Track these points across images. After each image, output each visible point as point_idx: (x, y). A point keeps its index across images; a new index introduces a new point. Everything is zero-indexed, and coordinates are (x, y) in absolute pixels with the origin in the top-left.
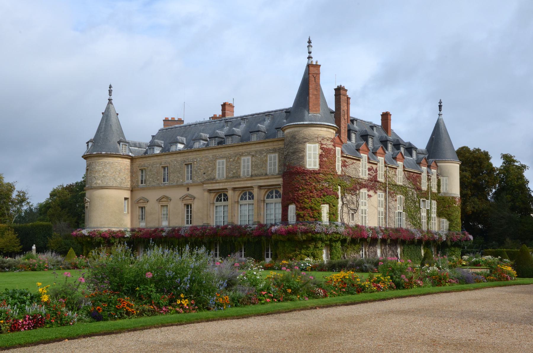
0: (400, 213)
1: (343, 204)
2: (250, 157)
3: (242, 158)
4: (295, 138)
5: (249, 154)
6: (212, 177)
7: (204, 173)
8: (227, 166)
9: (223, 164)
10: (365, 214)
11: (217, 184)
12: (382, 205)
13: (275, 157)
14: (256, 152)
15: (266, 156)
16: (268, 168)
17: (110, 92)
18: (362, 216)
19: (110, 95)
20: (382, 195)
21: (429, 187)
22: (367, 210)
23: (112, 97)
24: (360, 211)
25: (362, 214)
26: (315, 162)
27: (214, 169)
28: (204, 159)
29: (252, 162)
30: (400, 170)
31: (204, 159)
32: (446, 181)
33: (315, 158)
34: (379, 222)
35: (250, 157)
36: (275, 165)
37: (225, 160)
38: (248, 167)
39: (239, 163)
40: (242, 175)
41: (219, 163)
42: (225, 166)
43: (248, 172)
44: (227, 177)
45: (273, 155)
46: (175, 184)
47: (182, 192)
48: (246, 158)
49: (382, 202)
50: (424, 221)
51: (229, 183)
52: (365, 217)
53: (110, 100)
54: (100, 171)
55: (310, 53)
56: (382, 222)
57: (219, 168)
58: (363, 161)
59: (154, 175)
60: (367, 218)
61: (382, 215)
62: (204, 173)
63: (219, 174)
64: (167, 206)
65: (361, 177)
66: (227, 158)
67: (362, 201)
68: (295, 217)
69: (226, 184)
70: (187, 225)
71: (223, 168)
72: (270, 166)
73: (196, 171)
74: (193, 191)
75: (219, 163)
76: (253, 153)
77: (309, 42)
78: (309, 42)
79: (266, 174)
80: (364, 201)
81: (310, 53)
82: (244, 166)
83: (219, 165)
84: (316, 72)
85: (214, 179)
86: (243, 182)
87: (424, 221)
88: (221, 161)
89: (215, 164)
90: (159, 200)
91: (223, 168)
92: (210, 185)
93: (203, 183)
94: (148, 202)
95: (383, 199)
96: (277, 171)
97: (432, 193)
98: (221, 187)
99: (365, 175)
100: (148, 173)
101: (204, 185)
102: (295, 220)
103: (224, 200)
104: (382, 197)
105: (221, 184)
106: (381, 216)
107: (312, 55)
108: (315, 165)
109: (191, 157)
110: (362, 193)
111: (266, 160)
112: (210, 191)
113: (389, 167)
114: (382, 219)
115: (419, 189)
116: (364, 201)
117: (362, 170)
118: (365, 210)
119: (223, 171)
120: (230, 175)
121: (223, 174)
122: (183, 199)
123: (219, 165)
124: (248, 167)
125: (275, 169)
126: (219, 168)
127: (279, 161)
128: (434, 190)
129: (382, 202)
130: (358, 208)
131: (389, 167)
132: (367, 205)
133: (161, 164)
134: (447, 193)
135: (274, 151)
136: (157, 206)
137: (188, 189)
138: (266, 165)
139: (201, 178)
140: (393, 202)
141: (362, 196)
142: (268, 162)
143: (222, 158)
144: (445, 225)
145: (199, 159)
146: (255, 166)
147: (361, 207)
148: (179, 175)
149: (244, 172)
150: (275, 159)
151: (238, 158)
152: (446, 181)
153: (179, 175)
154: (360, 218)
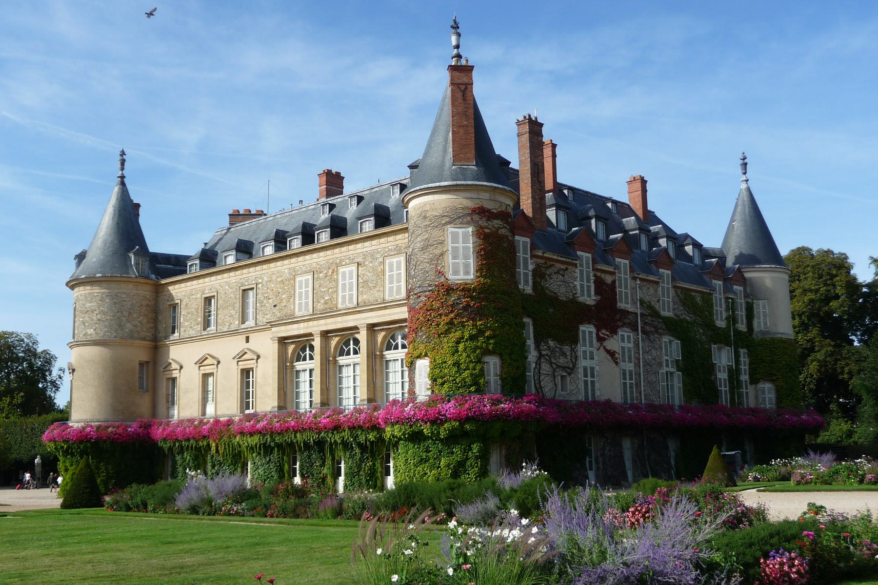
0: (672, 373)
1: (540, 356)
7: (275, 306)
10: (593, 376)
11: (295, 326)
12: (630, 357)
13: (399, 263)
14: (365, 256)
15: (384, 262)
17: (123, 162)
18: (586, 382)
19: (122, 169)
20: (629, 337)
21: (732, 319)
22: (597, 368)
24: (581, 371)
25: (586, 376)
26: (466, 266)
28: (274, 277)
30: (667, 285)
32: (764, 307)
33: (466, 257)
34: (625, 393)
39: (337, 281)
45: (395, 260)
47: (237, 344)
48: (346, 269)
49: (629, 351)
50: (724, 389)
51: (315, 323)
52: (593, 382)
56: (632, 392)
58: (582, 266)
60: (597, 385)
61: (631, 379)
62: (275, 306)
65: (581, 299)
67: (584, 348)
69: (311, 323)
75: (301, 282)
76: (360, 260)
80: (588, 349)
84: (465, 80)
85: (292, 315)
87: (723, 389)
90: (201, 362)
93: (272, 324)
95: (631, 345)
97: (737, 333)
98: (302, 332)
99: (589, 295)
104: (629, 342)
105: (302, 325)
106: (628, 381)
108: (467, 273)
110: (584, 332)
111: (383, 271)
112: (283, 341)
113: (641, 279)
114: (631, 387)
115: (709, 325)
116: (588, 349)
117: (582, 286)
118: (592, 369)
120: (320, 306)
122: (240, 357)
126: (301, 293)
128: (742, 327)
129: (629, 351)
130: (574, 365)
131: (641, 279)
132: (596, 358)
133: (203, 293)
134: (768, 332)
135: (398, 251)
139: (268, 317)
140: (653, 351)
141: (584, 340)
142: (387, 274)
143: (306, 272)
144: (767, 396)
145: (266, 279)
147: (583, 363)
148: (233, 312)
149: (344, 297)
152: (764, 307)
154: (582, 386)
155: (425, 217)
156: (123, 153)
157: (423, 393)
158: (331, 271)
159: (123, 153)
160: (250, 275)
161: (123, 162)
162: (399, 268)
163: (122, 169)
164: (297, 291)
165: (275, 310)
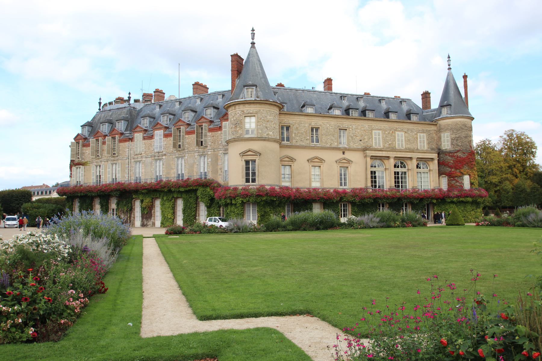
2: (403, 133)
3: (397, 133)
5: (402, 131)
6: (369, 145)
8: (383, 137)
9: (379, 135)
11: (380, 152)
13: (423, 136)
14: (408, 130)
15: (417, 134)
16: (419, 144)
19: (253, 39)
23: (255, 41)
27: (370, 138)
28: (359, 127)
29: (405, 137)
31: (359, 127)
36: (424, 143)
37: (380, 132)
38: (402, 141)
39: (395, 137)
40: (397, 147)
41: (375, 133)
43: (402, 145)
44: (384, 146)
45: (422, 135)
46: (328, 146)
47: (339, 155)
48: (400, 133)
51: (391, 153)
53: (253, 44)
54: (272, 122)
55: (449, 65)
57: (376, 138)
59: (302, 134)
63: (376, 143)
64: (320, 166)
66: (384, 130)
68: (469, 185)
69: (389, 153)
70: (341, 187)
71: (379, 138)
72: (420, 143)
73: (352, 137)
74: (349, 155)
75: (375, 133)
77: (449, 57)
78: (449, 57)
79: (418, 149)
81: (449, 65)
82: (398, 140)
83: (375, 135)
86: (404, 153)
88: (377, 132)
89: (371, 134)
91: (379, 138)
92: (373, 152)
94: (308, 160)
96: (426, 148)
100: (295, 132)
101: (367, 152)
102: (469, 187)
103: (378, 167)
105: (384, 152)
107: (451, 67)
112: (373, 158)
119: (379, 140)
120: (387, 145)
123: (375, 135)
125: (424, 146)
133: (310, 125)
135: (423, 132)
137: (344, 153)
138: (417, 141)
142: (419, 139)
146: (408, 141)
149: (399, 144)
151: (393, 132)
155: (466, 126)
156: (253, 30)
157: (444, 186)
158: (391, 132)
159: (253, 30)
160: (346, 123)
161: (253, 35)
162: (423, 138)
163: (253, 39)
164: (374, 136)
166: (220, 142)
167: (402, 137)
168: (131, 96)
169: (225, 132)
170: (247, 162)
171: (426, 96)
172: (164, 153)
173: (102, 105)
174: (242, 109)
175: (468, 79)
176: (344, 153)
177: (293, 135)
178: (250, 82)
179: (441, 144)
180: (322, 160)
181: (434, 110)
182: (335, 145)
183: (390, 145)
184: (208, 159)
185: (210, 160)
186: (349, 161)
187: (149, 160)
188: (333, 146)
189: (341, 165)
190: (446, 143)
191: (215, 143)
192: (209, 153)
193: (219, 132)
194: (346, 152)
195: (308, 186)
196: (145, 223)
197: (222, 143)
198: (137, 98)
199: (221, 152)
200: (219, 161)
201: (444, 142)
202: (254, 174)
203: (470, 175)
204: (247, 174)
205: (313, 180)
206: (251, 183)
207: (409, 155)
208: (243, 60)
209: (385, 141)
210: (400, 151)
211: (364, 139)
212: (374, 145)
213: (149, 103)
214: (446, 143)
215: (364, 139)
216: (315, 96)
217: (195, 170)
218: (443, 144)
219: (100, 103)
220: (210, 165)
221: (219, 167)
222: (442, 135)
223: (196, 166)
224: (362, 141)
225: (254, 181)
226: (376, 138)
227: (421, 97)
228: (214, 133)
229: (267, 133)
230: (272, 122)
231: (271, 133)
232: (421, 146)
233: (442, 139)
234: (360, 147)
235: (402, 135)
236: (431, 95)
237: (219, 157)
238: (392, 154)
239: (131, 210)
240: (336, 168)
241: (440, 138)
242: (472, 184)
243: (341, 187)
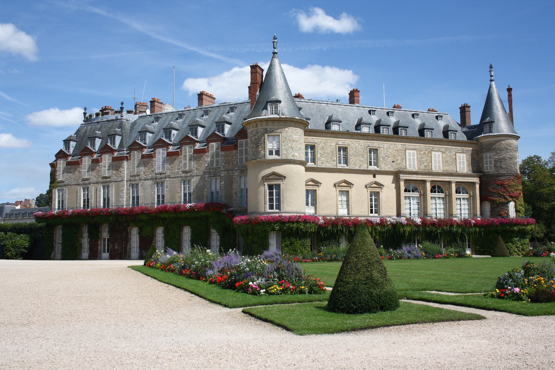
3: (433, 153)
4: (511, 146)
6: (403, 167)
7: (393, 162)
8: (417, 158)
9: (414, 156)
13: (463, 157)
29: (443, 158)
35: (440, 153)
36: (463, 164)
37: (415, 152)
38: (439, 163)
41: (410, 153)
42: (416, 157)
43: (439, 167)
45: (461, 155)
46: (357, 168)
47: (369, 178)
54: (297, 141)
57: (410, 159)
62: (393, 162)
71: (414, 159)
72: (460, 164)
73: (383, 158)
74: (380, 178)
75: (410, 153)
76: (443, 150)
77: (491, 67)
78: (491, 67)
82: (435, 161)
83: (409, 156)
88: (411, 152)
91: (414, 159)
100: (320, 152)
109: (375, 144)
120: (422, 167)
121: (414, 165)
124: (439, 163)
125: (464, 168)
127: (467, 161)
136: (334, 192)
137: (374, 177)
139: (389, 166)
146: (445, 162)
148: (363, 159)
149: (435, 166)
150: (463, 159)
151: (429, 152)
153: (363, 159)
158: (427, 152)
162: (463, 159)
164: (407, 157)
165: (393, 164)
166: (235, 163)
167: (439, 158)
168: (123, 106)
169: (241, 151)
170: (271, 187)
171: (464, 110)
172: (168, 174)
173: (87, 115)
174: (265, 127)
175: (513, 92)
176: (374, 177)
177: (319, 156)
178: (274, 97)
179: (483, 166)
180: (349, 184)
181: (475, 127)
182: (364, 167)
183: (425, 166)
184: (220, 182)
185: (223, 183)
186: (380, 185)
187: (149, 182)
188: (362, 168)
189: (372, 190)
190: (489, 165)
191: (229, 164)
192: (222, 175)
193: (234, 151)
194: (377, 176)
195: (335, 214)
196: (144, 255)
197: (237, 163)
198: (130, 109)
199: (236, 174)
200: (234, 184)
201: (487, 164)
202: (279, 200)
203: (515, 202)
204: (271, 200)
205: (340, 206)
206: (275, 210)
207: (447, 179)
208: (263, 70)
209: (420, 162)
210: (438, 174)
211: (397, 160)
212: (408, 167)
213: (144, 114)
214: (489, 165)
215: (397, 160)
216: (340, 110)
217: (205, 194)
218: (485, 166)
219: (85, 114)
220: (223, 188)
221: (234, 191)
222: (484, 155)
223: (206, 190)
224: (395, 163)
225: (278, 207)
226: (410, 159)
227: (459, 110)
228: (227, 153)
229: (292, 154)
230: (297, 141)
231: (297, 154)
232: (460, 167)
233: (485, 160)
234: (392, 169)
235: (439, 155)
236: (471, 109)
237: (234, 180)
238: (428, 178)
239: (127, 240)
240: (366, 194)
241: (482, 159)
242: (517, 211)
243: (371, 215)
